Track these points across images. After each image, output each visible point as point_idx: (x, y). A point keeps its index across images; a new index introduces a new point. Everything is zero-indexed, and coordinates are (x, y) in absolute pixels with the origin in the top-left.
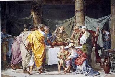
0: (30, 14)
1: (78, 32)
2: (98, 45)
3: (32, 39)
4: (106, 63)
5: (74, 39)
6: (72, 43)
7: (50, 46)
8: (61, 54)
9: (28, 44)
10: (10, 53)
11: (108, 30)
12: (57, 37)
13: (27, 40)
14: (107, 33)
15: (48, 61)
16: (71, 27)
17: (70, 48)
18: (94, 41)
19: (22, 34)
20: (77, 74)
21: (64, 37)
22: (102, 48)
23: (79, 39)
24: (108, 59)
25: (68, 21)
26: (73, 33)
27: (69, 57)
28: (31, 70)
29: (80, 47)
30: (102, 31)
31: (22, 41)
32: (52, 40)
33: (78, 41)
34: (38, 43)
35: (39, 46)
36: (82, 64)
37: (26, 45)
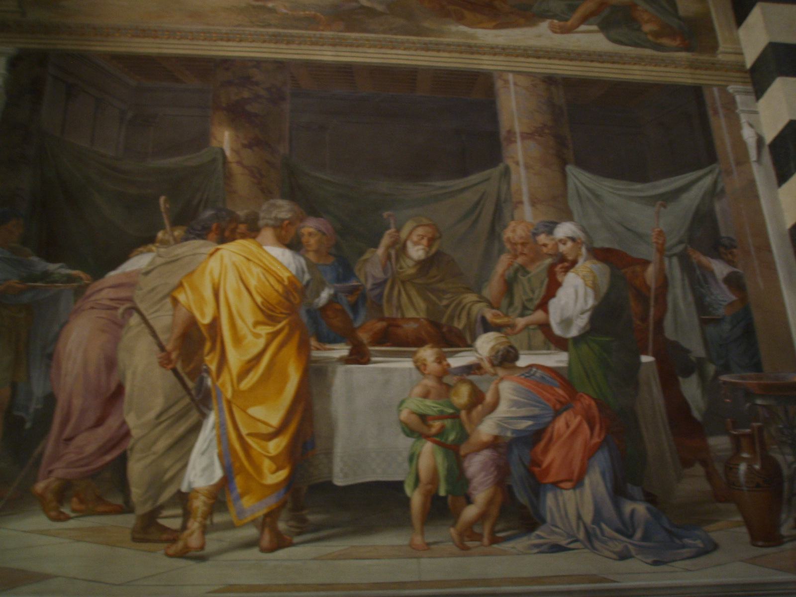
0: (203, 139)
1: (533, 261)
2: (676, 346)
3: (208, 294)
4: (743, 467)
5: (511, 304)
6: (498, 328)
7: (342, 351)
8: (430, 406)
9: (178, 331)
10: (39, 389)
11: (722, 250)
12: (392, 288)
13: (175, 301)
14: (720, 269)
15: (329, 453)
16: (484, 224)
17: (486, 365)
18: (645, 319)
19: (139, 262)
20: (556, 548)
21: (442, 286)
22: (699, 360)
23: (543, 306)
24: (750, 436)
25: (462, 190)
26: (502, 265)
27: (487, 429)
28: (194, 525)
29: (557, 359)
30: (684, 258)
31: (142, 307)
32: (355, 307)
33: (539, 315)
34: (257, 324)
35: (262, 342)
36: (583, 472)
37: (163, 337)
